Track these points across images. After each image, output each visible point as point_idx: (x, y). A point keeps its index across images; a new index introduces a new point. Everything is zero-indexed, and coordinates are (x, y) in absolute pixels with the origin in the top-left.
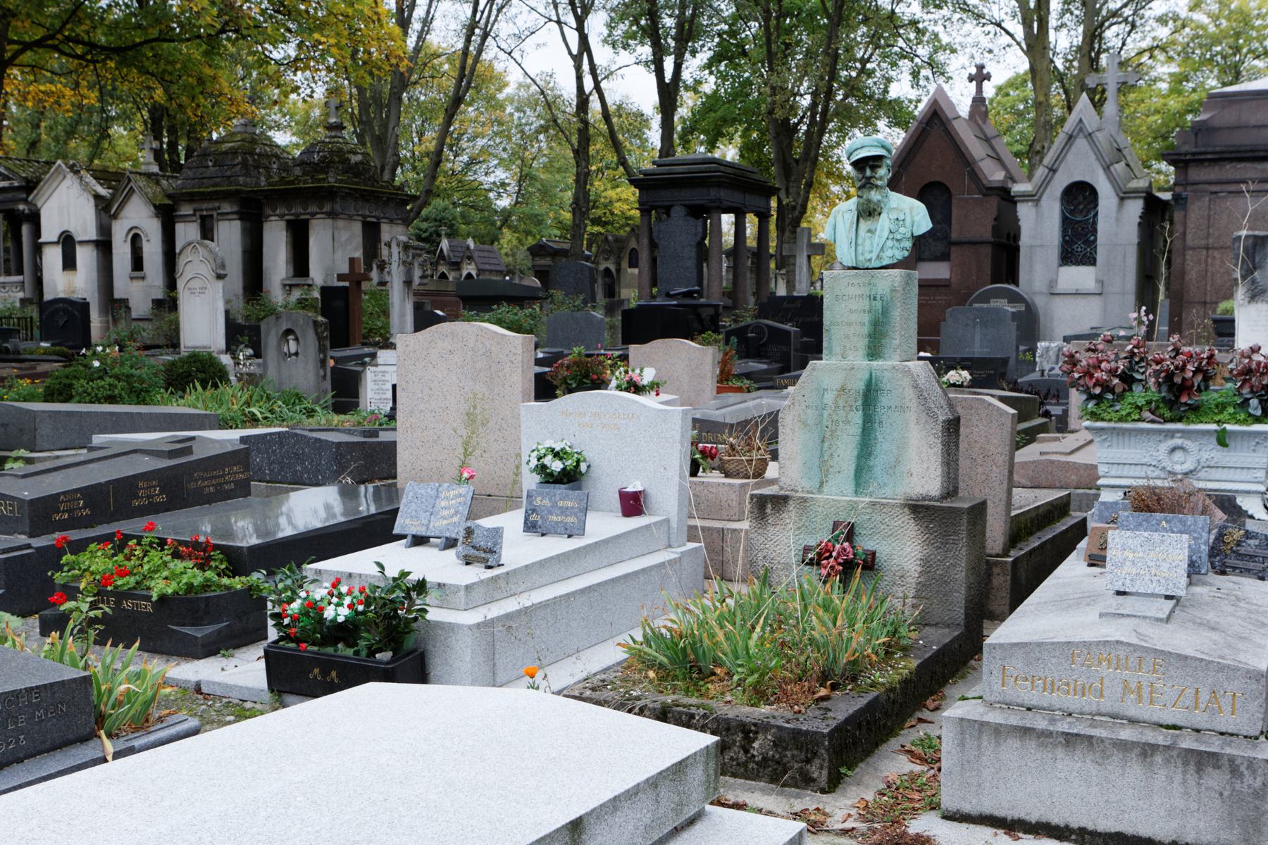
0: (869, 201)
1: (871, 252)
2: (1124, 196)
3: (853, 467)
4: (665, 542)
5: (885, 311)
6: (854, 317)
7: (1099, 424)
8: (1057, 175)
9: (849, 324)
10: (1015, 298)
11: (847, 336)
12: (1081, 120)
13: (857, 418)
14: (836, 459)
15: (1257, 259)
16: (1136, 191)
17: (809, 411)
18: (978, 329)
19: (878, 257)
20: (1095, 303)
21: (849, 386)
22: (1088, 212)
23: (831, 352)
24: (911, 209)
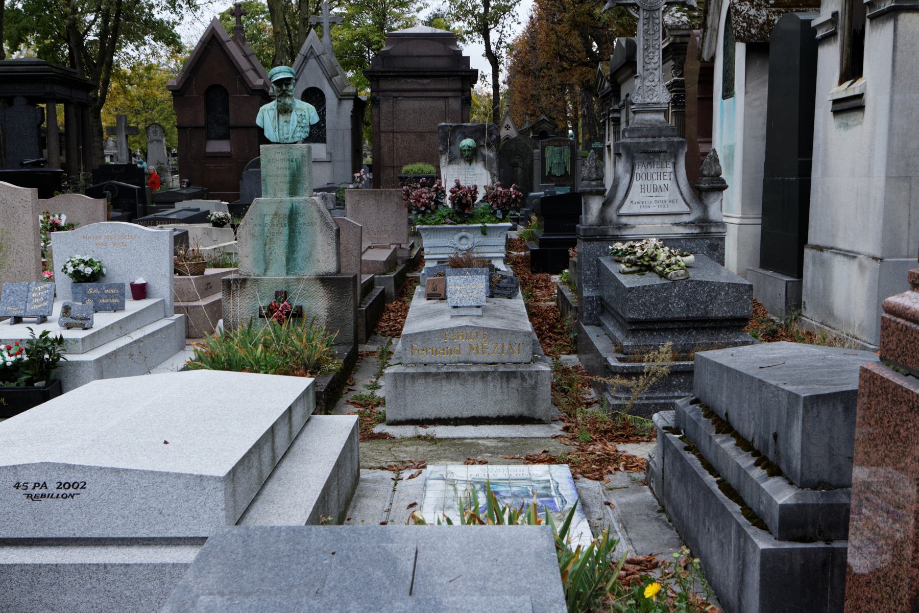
0: (285, 104)
2: (341, 98)
4: (163, 315)
5: (299, 168)
7: (425, 226)
9: (277, 176)
11: (276, 183)
13: (285, 231)
16: (348, 95)
17: (256, 228)
19: (293, 137)
20: (327, 168)
21: (280, 212)
23: (267, 193)
24: (308, 109)
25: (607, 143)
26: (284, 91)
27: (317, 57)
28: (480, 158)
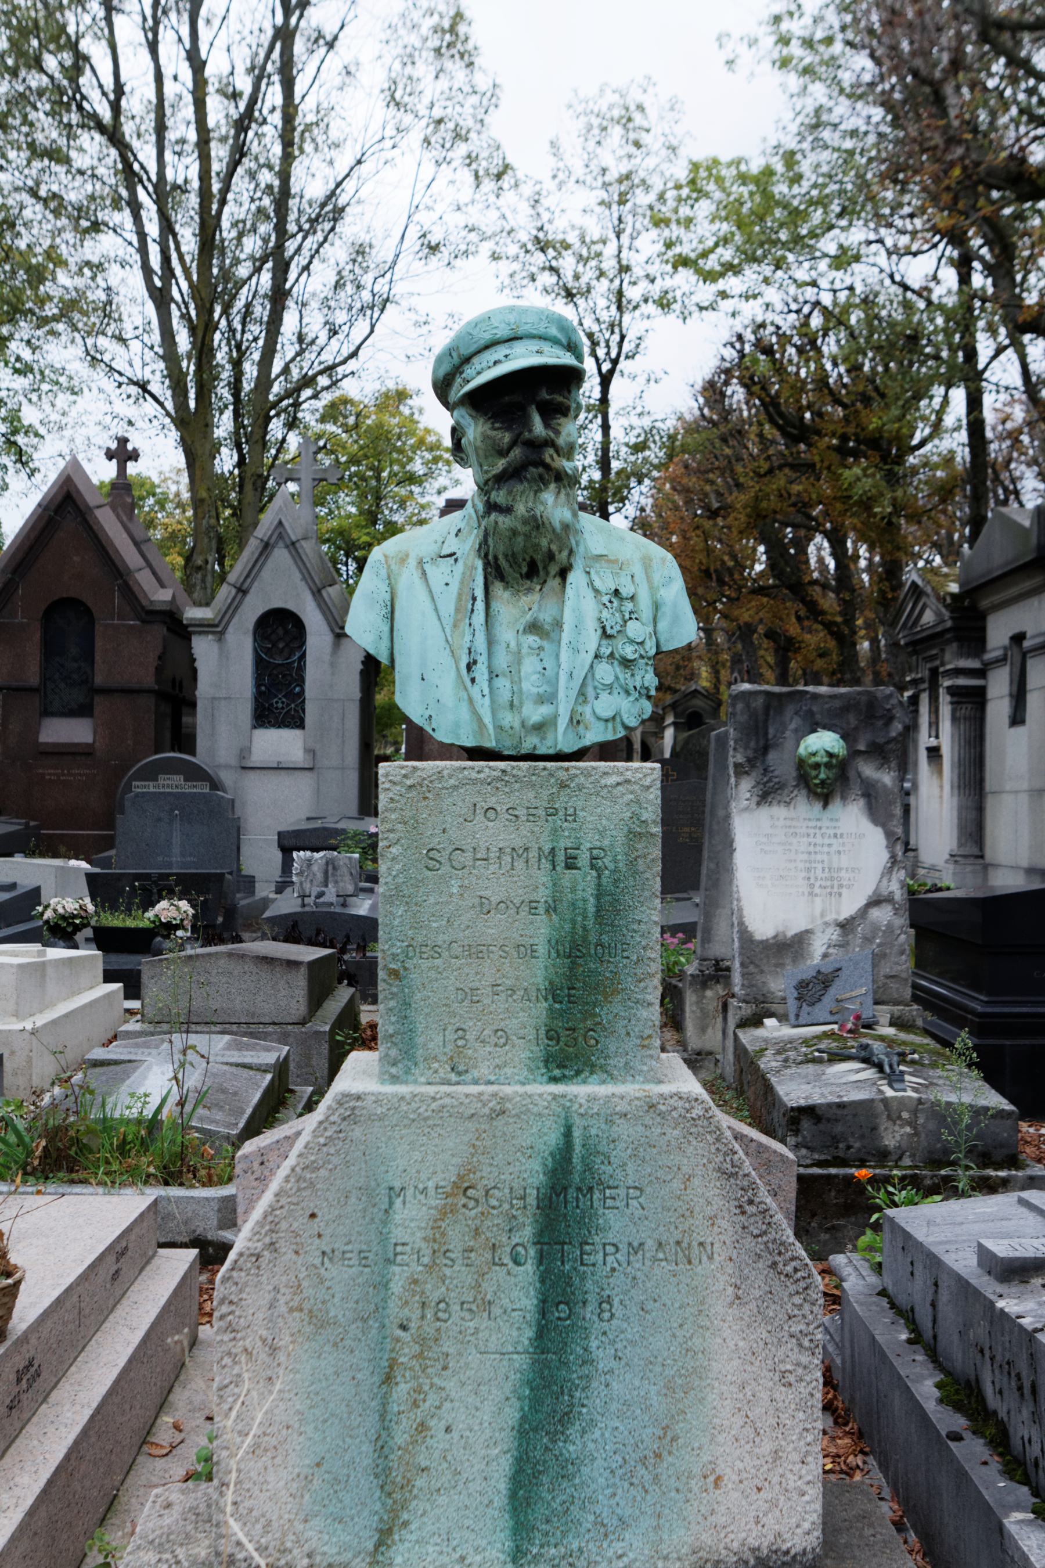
0: (536, 524)
1: (548, 698)
3: (502, 1468)
5: (609, 907)
6: (493, 928)
8: (249, 599)
9: (476, 952)
10: (196, 773)
11: (470, 995)
12: (280, 523)
13: (518, 1289)
14: (438, 1440)
15: (771, 731)
17: (336, 1273)
18: (177, 825)
19: (575, 722)
20: (304, 783)
21: (487, 1176)
22: (292, 653)
24: (647, 563)
25: (925, 740)
26: (537, 446)
27: (292, 546)
28: (856, 789)
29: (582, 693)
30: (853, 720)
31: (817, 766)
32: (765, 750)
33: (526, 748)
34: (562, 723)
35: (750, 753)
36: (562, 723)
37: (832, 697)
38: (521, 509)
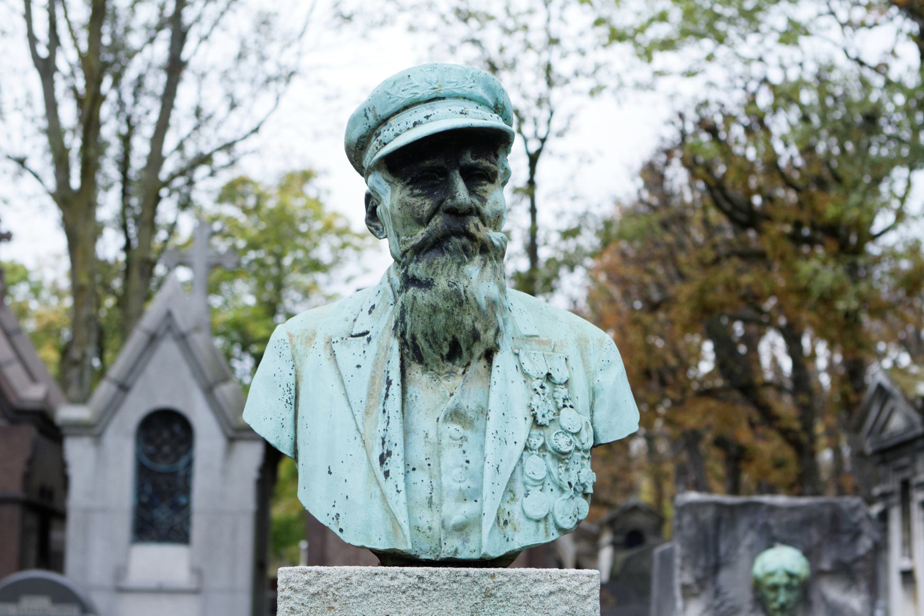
0: (459, 300)
1: (471, 495)
12: (169, 314)
15: (723, 548)
19: (502, 522)
22: (178, 457)
24: (582, 344)
26: (459, 214)
27: (182, 339)
29: (510, 490)
30: (815, 535)
31: (775, 588)
32: (715, 568)
33: (446, 552)
34: (488, 522)
35: (699, 573)
36: (488, 522)
37: (792, 509)
38: (442, 283)
